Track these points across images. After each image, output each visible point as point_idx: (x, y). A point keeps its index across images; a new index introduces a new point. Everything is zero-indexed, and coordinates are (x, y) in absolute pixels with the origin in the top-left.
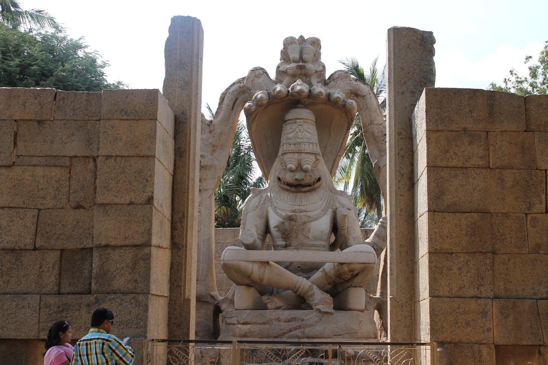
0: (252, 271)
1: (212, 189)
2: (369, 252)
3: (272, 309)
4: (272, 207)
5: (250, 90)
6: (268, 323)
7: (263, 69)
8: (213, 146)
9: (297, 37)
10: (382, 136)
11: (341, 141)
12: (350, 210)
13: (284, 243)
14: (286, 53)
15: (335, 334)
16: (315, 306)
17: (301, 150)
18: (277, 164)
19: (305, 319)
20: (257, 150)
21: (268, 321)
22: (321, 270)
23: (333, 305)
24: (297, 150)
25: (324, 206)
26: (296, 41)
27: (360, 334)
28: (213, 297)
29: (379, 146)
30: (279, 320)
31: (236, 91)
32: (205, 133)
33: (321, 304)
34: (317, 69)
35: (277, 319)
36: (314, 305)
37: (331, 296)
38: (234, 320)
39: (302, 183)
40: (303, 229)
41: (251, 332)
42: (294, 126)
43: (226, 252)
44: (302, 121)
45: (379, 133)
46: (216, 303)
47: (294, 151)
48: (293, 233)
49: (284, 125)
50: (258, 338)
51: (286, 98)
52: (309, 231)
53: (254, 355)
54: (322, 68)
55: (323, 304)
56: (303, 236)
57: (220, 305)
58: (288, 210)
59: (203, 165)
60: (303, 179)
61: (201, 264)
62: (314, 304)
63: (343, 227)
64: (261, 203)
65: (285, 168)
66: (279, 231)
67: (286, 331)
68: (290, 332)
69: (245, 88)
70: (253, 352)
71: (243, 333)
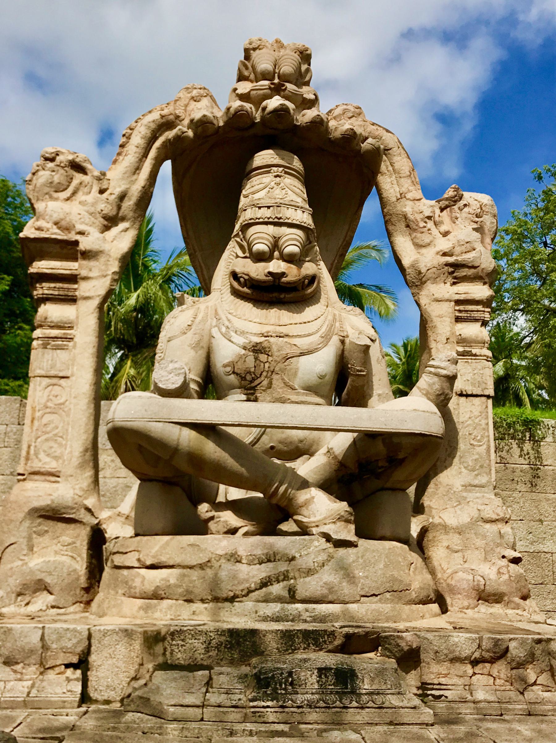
0: (178, 445)
1: (99, 296)
2: (432, 413)
3: (218, 533)
4: (219, 328)
5: (181, 121)
6: (209, 564)
7: (205, 89)
8: (106, 218)
9: (271, 40)
10: (422, 220)
11: (346, 227)
12: (372, 340)
13: (244, 397)
14: (249, 65)
15: (363, 594)
16: (317, 526)
17: (280, 218)
18: (232, 248)
19: (297, 555)
20: (191, 233)
21: (209, 561)
22: (323, 450)
23: (352, 527)
24: (274, 217)
25: (323, 330)
26: (269, 46)
27: (413, 593)
28: (89, 510)
29: (415, 237)
30: (236, 558)
31: (154, 121)
32: (90, 193)
33: (329, 523)
34: (304, 96)
35: (231, 556)
36: (314, 525)
37: (350, 505)
38: (131, 560)
39: (284, 280)
40: (283, 370)
41: (169, 586)
42: (267, 179)
43: (118, 403)
44: (281, 169)
45: (416, 215)
46: (96, 522)
47: (266, 220)
48: (262, 378)
49: (245, 181)
50: (185, 601)
51: (252, 131)
52: (295, 374)
53: (174, 645)
54: (313, 97)
55: (334, 522)
56: (283, 385)
57: (104, 526)
58: (254, 332)
59: (84, 249)
60: (283, 274)
61: (69, 443)
62: (314, 522)
63: (361, 371)
64: (197, 320)
65: (248, 255)
66: (234, 373)
67: (253, 585)
68: (261, 588)
69: (172, 117)
70: (173, 640)
71: (149, 588)
